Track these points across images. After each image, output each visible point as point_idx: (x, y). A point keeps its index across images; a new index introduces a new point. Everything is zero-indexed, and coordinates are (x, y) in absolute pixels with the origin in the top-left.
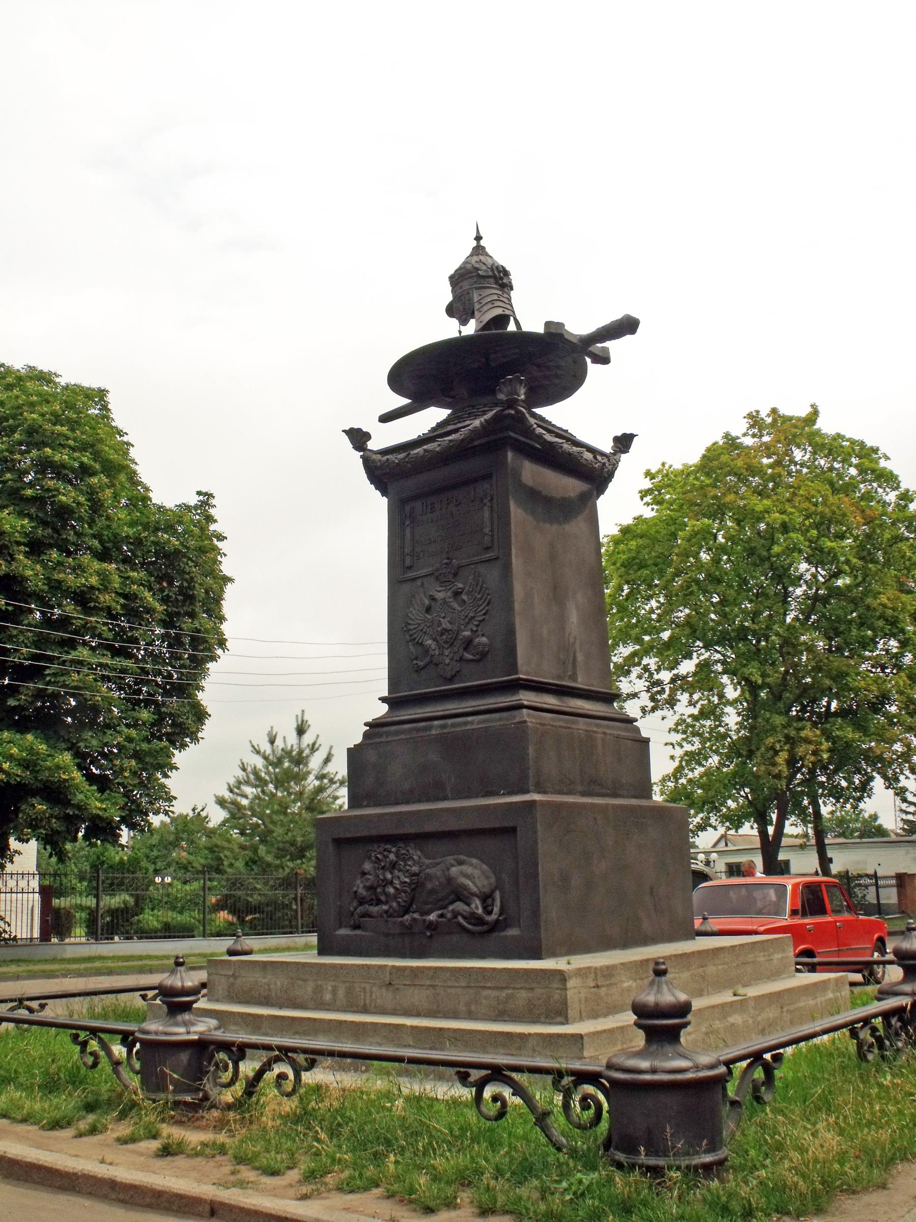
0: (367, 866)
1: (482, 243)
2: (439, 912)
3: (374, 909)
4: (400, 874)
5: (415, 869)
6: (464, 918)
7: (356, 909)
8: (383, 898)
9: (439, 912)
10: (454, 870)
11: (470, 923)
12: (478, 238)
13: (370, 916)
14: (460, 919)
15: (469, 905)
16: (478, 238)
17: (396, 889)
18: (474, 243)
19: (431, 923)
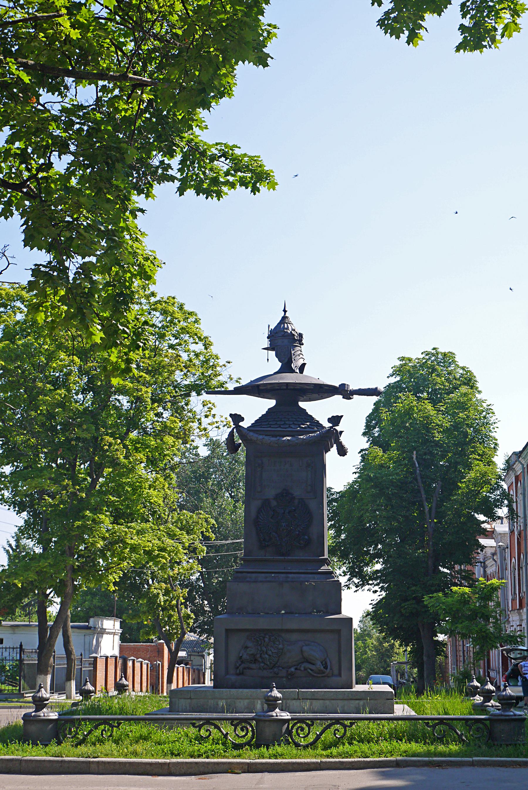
0: (250, 644)
1: (287, 315)
2: (295, 667)
3: (253, 666)
4: (272, 649)
5: (281, 646)
6: (311, 670)
7: (240, 665)
8: (260, 660)
9: (295, 667)
10: (305, 648)
11: (315, 673)
12: (285, 311)
13: (251, 669)
14: (309, 671)
15: (314, 664)
16: (285, 311)
17: (270, 656)
18: (283, 313)
19: (292, 672)
